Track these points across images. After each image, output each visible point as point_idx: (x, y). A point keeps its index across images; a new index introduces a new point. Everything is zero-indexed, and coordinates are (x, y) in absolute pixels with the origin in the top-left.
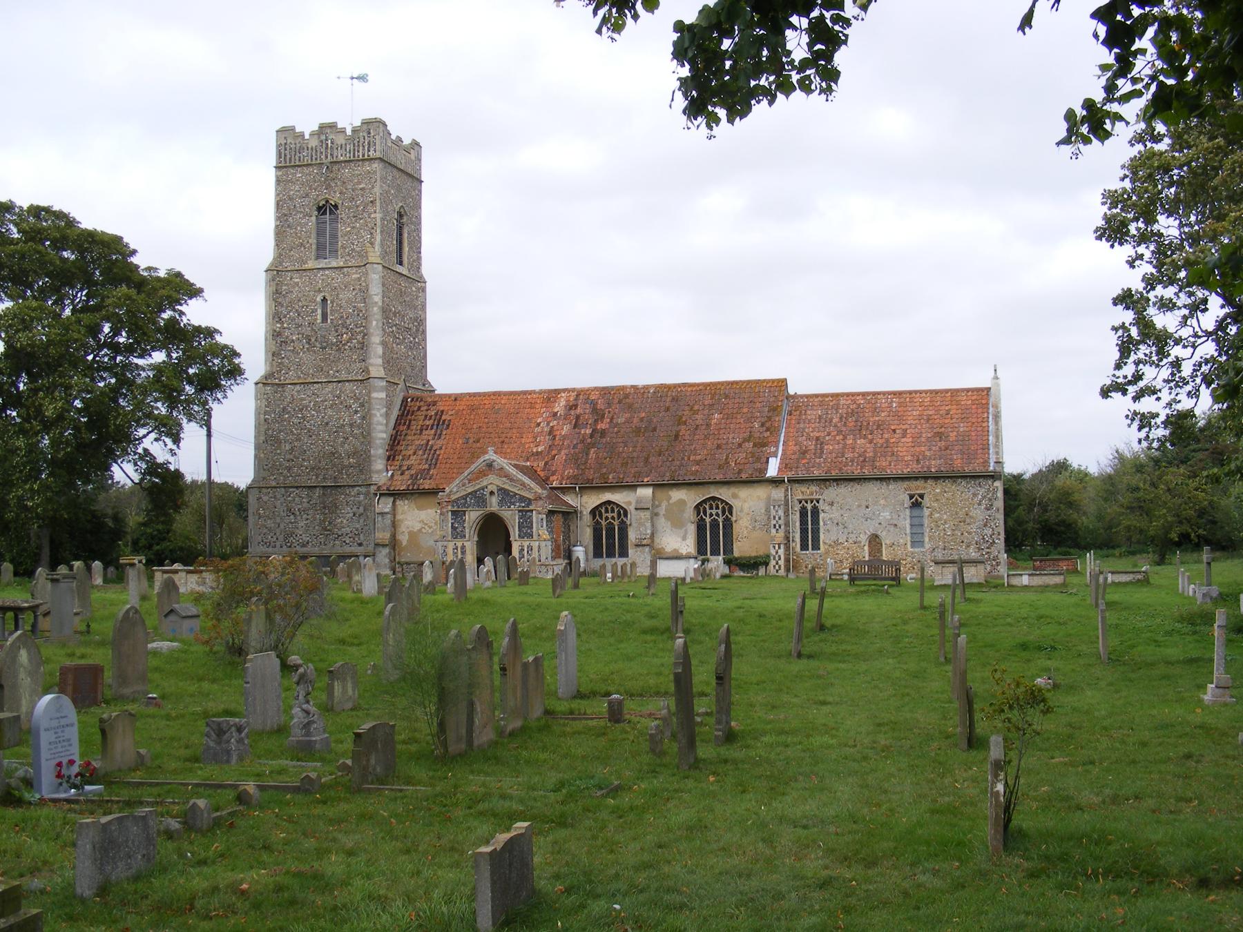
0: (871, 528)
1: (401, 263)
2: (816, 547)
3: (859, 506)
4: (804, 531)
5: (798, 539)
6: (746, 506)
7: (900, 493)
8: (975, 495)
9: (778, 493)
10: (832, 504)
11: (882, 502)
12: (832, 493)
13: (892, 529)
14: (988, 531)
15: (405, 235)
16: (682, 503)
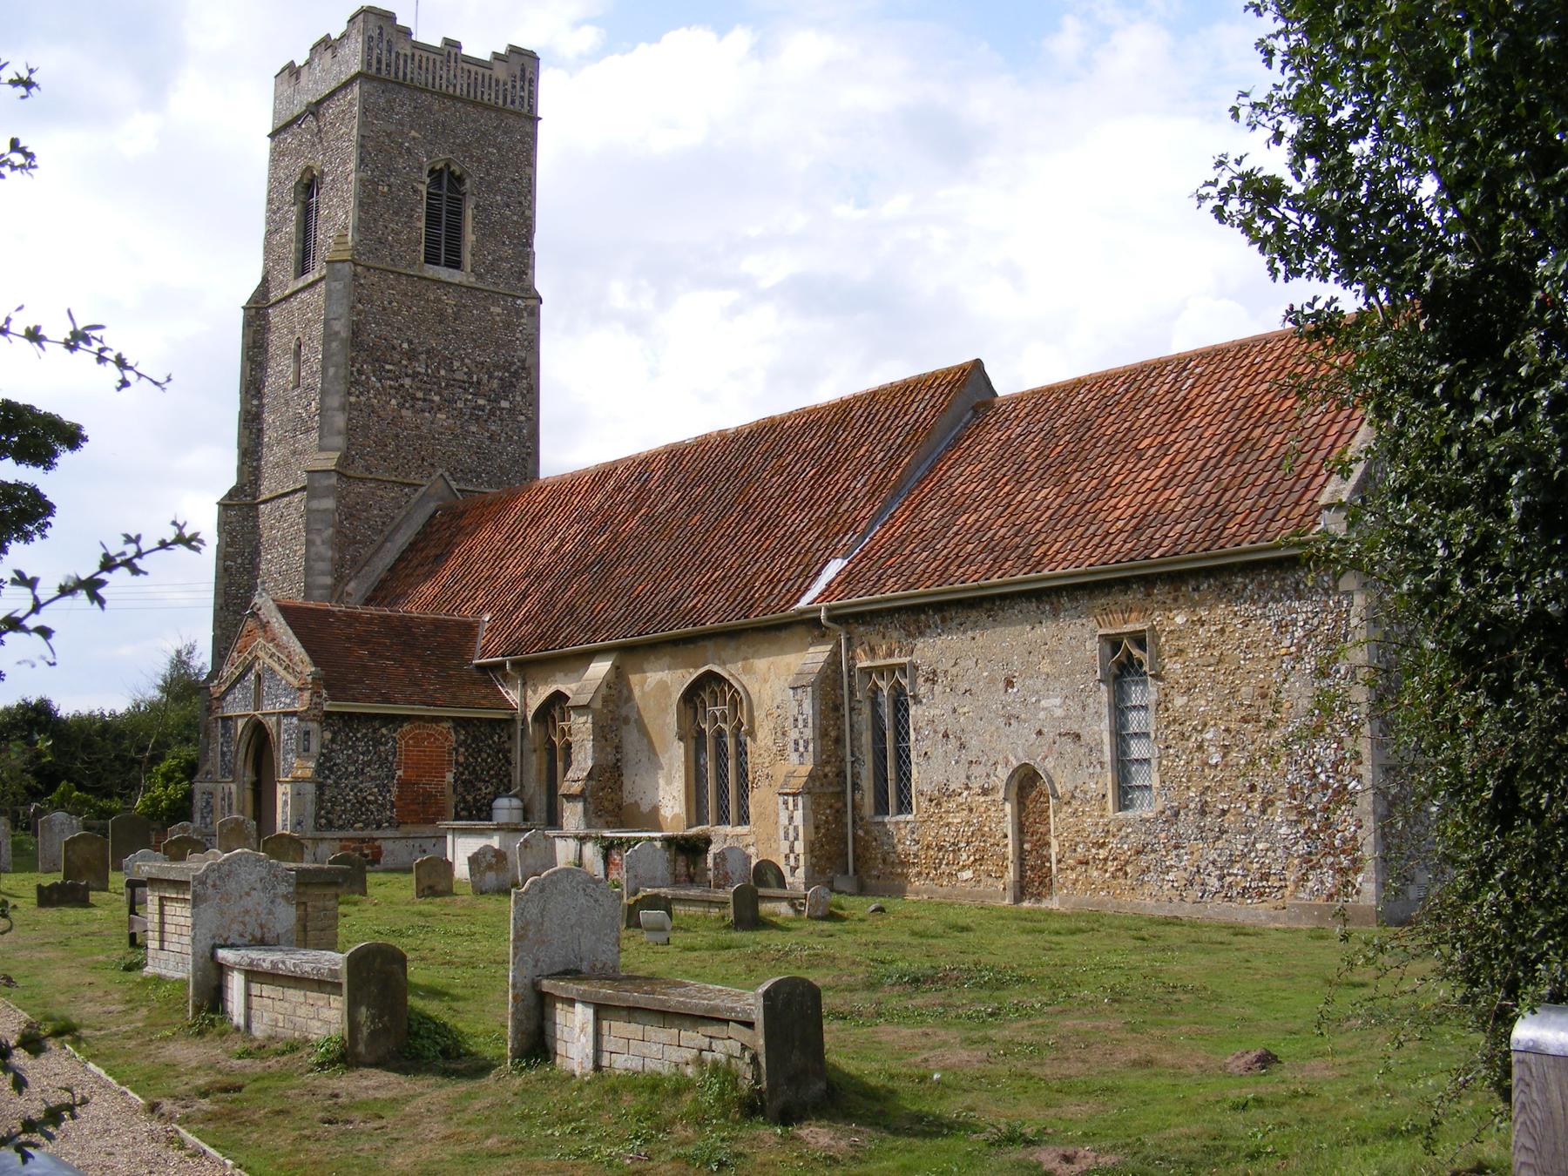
0: (1015, 749)
1: (456, 265)
2: (904, 806)
3: (992, 681)
4: (880, 756)
5: (867, 782)
6: (767, 693)
7: (1078, 638)
8: (1282, 627)
9: (816, 656)
10: (932, 679)
11: (1046, 667)
12: (931, 650)
13: (1069, 746)
14: (1325, 751)
15: (469, 213)
16: (663, 687)
